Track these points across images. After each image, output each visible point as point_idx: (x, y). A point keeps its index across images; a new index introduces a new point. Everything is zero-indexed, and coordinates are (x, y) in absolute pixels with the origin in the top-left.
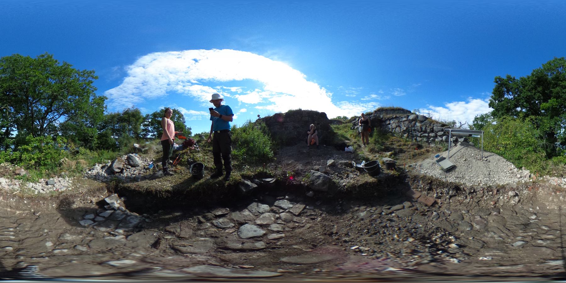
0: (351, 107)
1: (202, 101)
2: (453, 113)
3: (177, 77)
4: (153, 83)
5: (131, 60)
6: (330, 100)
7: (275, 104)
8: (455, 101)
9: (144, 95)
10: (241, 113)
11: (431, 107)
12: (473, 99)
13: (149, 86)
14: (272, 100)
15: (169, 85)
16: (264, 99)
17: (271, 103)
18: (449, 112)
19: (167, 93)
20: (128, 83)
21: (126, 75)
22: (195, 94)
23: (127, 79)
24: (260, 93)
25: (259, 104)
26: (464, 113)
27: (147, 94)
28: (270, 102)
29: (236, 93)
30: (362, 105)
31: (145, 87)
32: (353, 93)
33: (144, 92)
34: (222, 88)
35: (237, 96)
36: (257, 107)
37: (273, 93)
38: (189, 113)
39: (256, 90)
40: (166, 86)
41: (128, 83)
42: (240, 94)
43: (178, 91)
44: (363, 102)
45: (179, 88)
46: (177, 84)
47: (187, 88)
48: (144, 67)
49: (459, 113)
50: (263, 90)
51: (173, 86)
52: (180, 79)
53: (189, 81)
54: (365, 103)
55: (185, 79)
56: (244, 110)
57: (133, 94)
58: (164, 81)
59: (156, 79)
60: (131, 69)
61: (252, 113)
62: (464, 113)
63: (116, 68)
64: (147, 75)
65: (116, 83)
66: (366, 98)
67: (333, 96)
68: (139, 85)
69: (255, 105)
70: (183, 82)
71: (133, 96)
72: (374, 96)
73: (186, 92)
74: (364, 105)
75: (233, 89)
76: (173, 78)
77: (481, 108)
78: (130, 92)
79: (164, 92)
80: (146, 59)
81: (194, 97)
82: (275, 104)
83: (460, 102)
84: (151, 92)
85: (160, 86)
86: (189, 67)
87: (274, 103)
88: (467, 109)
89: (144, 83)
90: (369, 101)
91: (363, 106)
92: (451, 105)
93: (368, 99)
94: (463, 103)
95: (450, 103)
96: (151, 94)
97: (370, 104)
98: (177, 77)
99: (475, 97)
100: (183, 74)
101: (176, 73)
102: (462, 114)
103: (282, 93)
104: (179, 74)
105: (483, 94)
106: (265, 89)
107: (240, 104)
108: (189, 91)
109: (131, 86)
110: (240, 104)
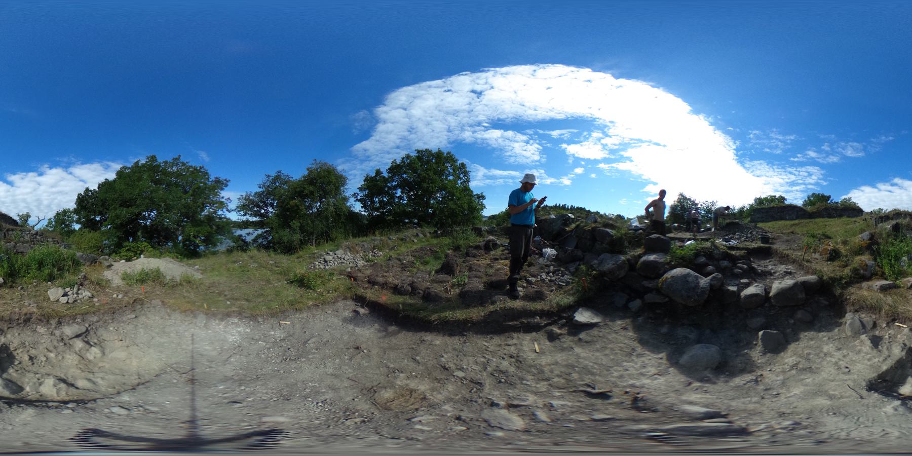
7: (631, 161)
14: (625, 154)
15: (449, 131)
16: (612, 152)
17: (622, 159)
19: (450, 143)
24: (603, 141)
25: (606, 161)
28: (622, 156)
36: (602, 166)
37: (626, 141)
40: (446, 133)
45: (467, 135)
51: (457, 132)
52: (466, 120)
53: (479, 124)
55: (471, 121)
61: (593, 176)
69: (596, 162)
70: (471, 126)
73: (479, 141)
79: (444, 142)
82: (631, 161)
84: (425, 143)
87: (629, 159)
106: (611, 132)
108: (482, 139)
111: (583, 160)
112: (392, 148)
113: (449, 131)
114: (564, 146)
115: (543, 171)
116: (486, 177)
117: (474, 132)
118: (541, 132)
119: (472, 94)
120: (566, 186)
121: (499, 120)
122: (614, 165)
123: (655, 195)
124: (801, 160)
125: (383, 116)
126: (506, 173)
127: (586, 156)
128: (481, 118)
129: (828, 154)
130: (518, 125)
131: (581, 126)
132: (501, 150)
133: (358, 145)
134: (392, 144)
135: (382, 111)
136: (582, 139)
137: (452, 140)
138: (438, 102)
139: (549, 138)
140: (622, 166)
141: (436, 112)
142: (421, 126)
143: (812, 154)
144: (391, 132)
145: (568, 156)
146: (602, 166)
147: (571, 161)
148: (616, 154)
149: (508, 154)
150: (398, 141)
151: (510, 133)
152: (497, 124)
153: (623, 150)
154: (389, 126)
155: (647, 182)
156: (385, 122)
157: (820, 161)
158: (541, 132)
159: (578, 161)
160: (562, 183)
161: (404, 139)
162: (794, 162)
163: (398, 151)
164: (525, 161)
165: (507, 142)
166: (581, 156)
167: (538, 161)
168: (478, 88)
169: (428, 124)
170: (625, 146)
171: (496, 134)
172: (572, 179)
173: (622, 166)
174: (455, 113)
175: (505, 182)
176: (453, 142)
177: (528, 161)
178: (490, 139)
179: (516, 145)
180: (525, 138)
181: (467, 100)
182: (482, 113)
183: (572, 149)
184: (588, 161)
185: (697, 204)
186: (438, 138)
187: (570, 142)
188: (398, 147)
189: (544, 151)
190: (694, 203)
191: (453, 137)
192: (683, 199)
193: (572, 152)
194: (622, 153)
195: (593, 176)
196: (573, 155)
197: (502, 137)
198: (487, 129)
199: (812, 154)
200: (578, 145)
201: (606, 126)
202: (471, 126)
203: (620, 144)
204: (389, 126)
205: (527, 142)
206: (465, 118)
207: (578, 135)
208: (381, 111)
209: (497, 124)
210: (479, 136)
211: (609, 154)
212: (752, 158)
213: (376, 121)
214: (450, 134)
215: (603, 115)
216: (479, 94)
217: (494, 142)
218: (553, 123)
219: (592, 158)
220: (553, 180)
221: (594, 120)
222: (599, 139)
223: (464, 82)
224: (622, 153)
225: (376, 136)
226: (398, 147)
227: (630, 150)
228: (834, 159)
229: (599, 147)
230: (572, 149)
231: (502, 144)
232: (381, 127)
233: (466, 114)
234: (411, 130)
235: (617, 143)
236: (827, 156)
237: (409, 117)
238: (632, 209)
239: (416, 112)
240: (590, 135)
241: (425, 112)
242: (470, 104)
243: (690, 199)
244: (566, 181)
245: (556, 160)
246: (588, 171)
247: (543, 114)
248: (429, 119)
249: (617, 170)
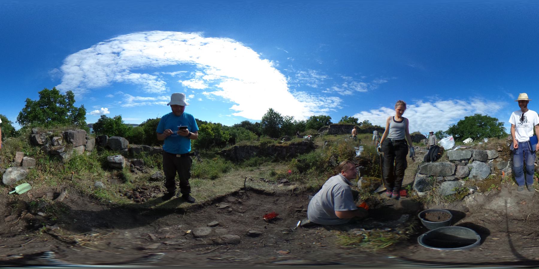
7: (223, 90)
16: (211, 85)
25: (207, 90)
28: (216, 87)
40: (105, 77)
51: (112, 76)
69: (201, 91)
82: (223, 90)
87: (221, 89)
108: (128, 79)
113: (107, 76)
114: (180, 81)
117: (122, 75)
119: (113, 55)
122: (212, 93)
124: (329, 92)
125: (68, 70)
127: (195, 87)
129: (346, 89)
132: (141, 85)
134: (75, 86)
135: (65, 68)
138: (96, 61)
140: (217, 93)
143: (336, 89)
144: (73, 79)
145: (184, 88)
146: (205, 93)
149: (146, 87)
151: (145, 75)
156: (68, 74)
157: (341, 93)
161: (82, 82)
162: (324, 93)
163: (79, 89)
168: (116, 50)
170: (218, 81)
173: (217, 93)
174: (108, 66)
176: (111, 82)
177: (159, 91)
179: (150, 82)
180: (155, 77)
184: (196, 90)
188: (79, 87)
193: (186, 85)
194: (216, 85)
196: (187, 87)
199: (336, 89)
204: (72, 76)
205: (157, 80)
208: (64, 68)
210: (126, 78)
211: (209, 86)
212: (299, 90)
213: (62, 73)
216: (118, 54)
217: (136, 81)
219: (199, 88)
223: (104, 48)
224: (216, 85)
228: (348, 93)
229: (202, 82)
231: (142, 81)
232: (66, 77)
233: (115, 66)
234: (84, 77)
236: (345, 91)
239: (86, 67)
241: (91, 66)
242: (114, 60)
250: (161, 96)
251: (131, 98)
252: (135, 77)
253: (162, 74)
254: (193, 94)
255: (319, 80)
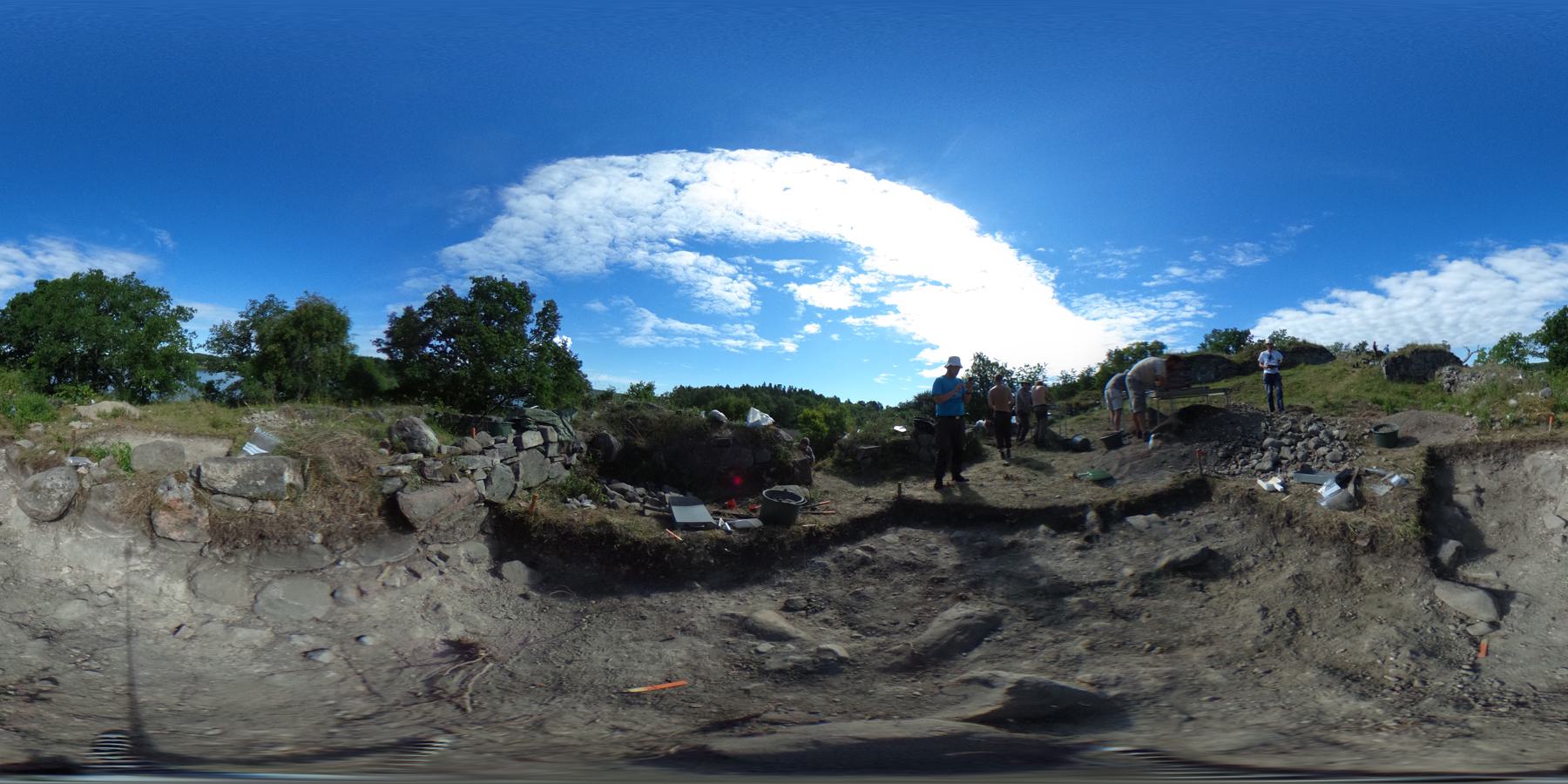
0: (1116, 311)
1: (699, 295)
2: (1398, 305)
3: (635, 226)
4: (574, 239)
5: (517, 174)
6: (1049, 291)
7: (897, 312)
8: (1401, 271)
9: (550, 267)
10: (807, 335)
11: (1336, 293)
12: (1450, 260)
13: (562, 244)
14: (888, 300)
15: (613, 245)
16: (867, 296)
17: (884, 309)
18: (1386, 303)
19: (608, 266)
20: (509, 234)
21: (499, 209)
22: (680, 275)
23: (502, 222)
24: (854, 280)
25: (856, 312)
26: (1427, 300)
27: (557, 265)
28: (882, 304)
29: (788, 277)
30: (1144, 301)
31: (551, 246)
32: (1116, 269)
33: (550, 259)
34: (750, 263)
35: (792, 286)
36: (849, 320)
37: (889, 279)
38: (665, 326)
39: (842, 269)
41: (509, 234)
42: (800, 282)
43: (634, 264)
44: (1149, 292)
45: (640, 256)
46: (635, 246)
47: (658, 259)
48: (552, 196)
49: (1414, 302)
50: (860, 271)
51: (624, 249)
52: (644, 230)
53: (663, 240)
54: (1155, 295)
55: (652, 233)
56: (812, 328)
57: (520, 263)
58: (600, 235)
59: (581, 228)
60: (518, 197)
61: (835, 337)
62: (1427, 300)
63: (474, 193)
64: (559, 216)
65: (471, 231)
66: (1157, 280)
67: (1057, 281)
68: (535, 239)
69: (841, 314)
70: (649, 241)
71: (519, 268)
72: (1177, 271)
73: (656, 269)
74: (1151, 301)
75: (781, 265)
76: (623, 228)
77: (1474, 284)
78: (511, 255)
79: (600, 264)
80: (555, 173)
81: (679, 284)
82: (897, 312)
83: (1416, 273)
85: (590, 249)
86: (661, 202)
88: (1434, 289)
89: (551, 235)
90: (1164, 290)
91: (1147, 306)
92: (1389, 283)
93: (1160, 282)
94: (1424, 273)
95: (1387, 276)
96: (568, 267)
97: (1168, 297)
98: (635, 226)
99: (1457, 254)
100: (649, 219)
101: (631, 215)
102: (1421, 305)
103: (911, 279)
104: (640, 218)
105: (1476, 244)
107: (800, 310)
108: (664, 265)
109: (515, 242)
110: (800, 310)
111: (820, 310)
112: (511, 262)
115: (752, 328)
116: (657, 331)
117: (652, 252)
118: (759, 261)
120: (788, 354)
121: (698, 235)
122: (868, 319)
123: (936, 365)
126: (690, 327)
127: (826, 305)
128: (671, 228)
130: (723, 247)
131: (822, 254)
133: (452, 248)
136: (822, 276)
137: (612, 262)
139: (770, 273)
140: (882, 321)
141: (601, 210)
142: (569, 232)
146: (849, 320)
147: (800, 312)
148: (872, 304)
150: (523, 252)
151: (709, 260)
152: (694, 243)
153: (885, 293)
154: (515, 223)
155: (920, 346)
158: (759, 261)
159: (811, 313)
160: (781, 348)
161: (533, 248)
164: (726, 309)
165: (702, 275)
166: (817, 305)
167: (747, 310)
169: (581, 228)
170: (887, 286)
171: (688, 258)
172: (800, 343)
173: (882, 321)
175: (688, 343)
178: (675, 267)
179: (716, 281)
180: (731, 269)
181: (657, 196)
182: (674, 224)
183: (804, 292)
184: (829, 313)
185: (1010, 373)
186: (592, 254)
187: (801, 281)
189: (760, 294)
190: (1005, 372)
191: (615, 256)
192: (982, 364)
193: (803, 297)
194: (882, 299)
195: (835, 337)
197: (695, 265)
198: (674, 248)
200: (814, 286)
201: (860, 255)
202: (649, 241)
203: (880, 285)
205: (734, 278)
206: (644, 227)
207: (815, 269)
209: (694, 243)
214: (613, 251)
215: (856, 237)
217: (681, 272)
218: (780, 248)
219: (835, 308)
220: (767, 343)
221: (844, 244)
222: (848, 277)
224: (882, 299)
225: (488, 238)
226: (520, 263)
227: (893, 293)
229: (848, 288)
230: (804, 292)
231: (694, 277)
235: (874, 282)
237: (553, 210)
238: (895, 389)
240: (835, 271)
243: (996, 365)
244: (789, 346)
245: (775, 310)
246: (826, 329)
247: (767, 230)
248: (587, 220)
249: (874, 328)
250: (733, 322)
251: (652, 320)
252: (684, 261)
253: (750, 263)
254: (817, 321)
255: (1127, 258)
